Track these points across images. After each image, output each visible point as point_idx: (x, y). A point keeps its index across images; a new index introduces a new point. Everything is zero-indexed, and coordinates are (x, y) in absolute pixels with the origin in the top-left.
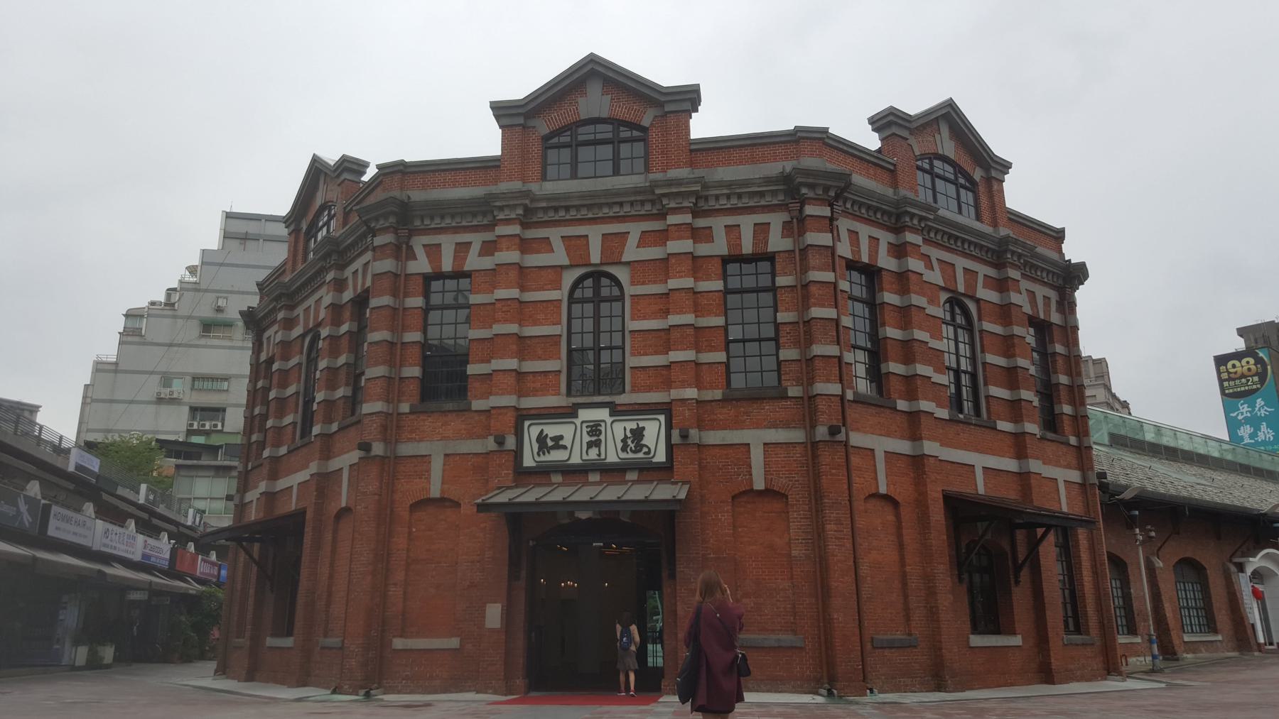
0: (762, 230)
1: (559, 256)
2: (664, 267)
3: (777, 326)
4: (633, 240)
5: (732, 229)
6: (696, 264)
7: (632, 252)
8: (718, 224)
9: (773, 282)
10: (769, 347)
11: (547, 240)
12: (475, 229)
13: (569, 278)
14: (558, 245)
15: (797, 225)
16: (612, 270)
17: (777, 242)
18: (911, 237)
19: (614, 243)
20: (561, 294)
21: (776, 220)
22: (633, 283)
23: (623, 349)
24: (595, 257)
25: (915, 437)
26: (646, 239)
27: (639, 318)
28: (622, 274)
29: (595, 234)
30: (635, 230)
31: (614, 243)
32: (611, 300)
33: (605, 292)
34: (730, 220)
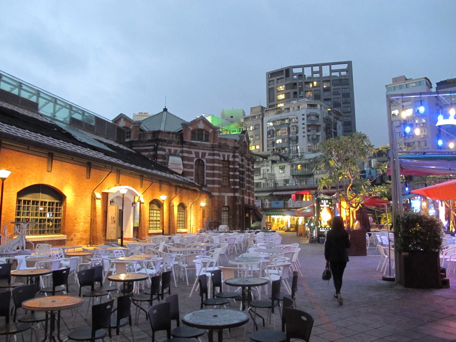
0: (229, 156)
1: (193, 155)
2: (213, 161)
3: (229, 175)
4: (207, 154)
5: (224, 156)
6: (219, 162)
7: (207, 157)
8: (221, 154)
9: (229, 166)
10: (227, 178)
11: (191, 152)
12: (179, 147)
13: (195, 160)
14: (194, 153)
15: (234, 157)
16: (202, 159)
17: (231, 159)
18: (244, 158)
19: (204, 155)
20: (194, 163)
21: (231, 154)
22: (207, 163)
23: (204, 176)
24: (200, 157)
25: (243, 194)
26: (210, 154)
27: (208, 170)
28: (204, 161)
29: (200, 152)
30: (207, 152)
31: (204, 155)
32: (201, 165)
33: (200, 163)
34: (224, 153)
